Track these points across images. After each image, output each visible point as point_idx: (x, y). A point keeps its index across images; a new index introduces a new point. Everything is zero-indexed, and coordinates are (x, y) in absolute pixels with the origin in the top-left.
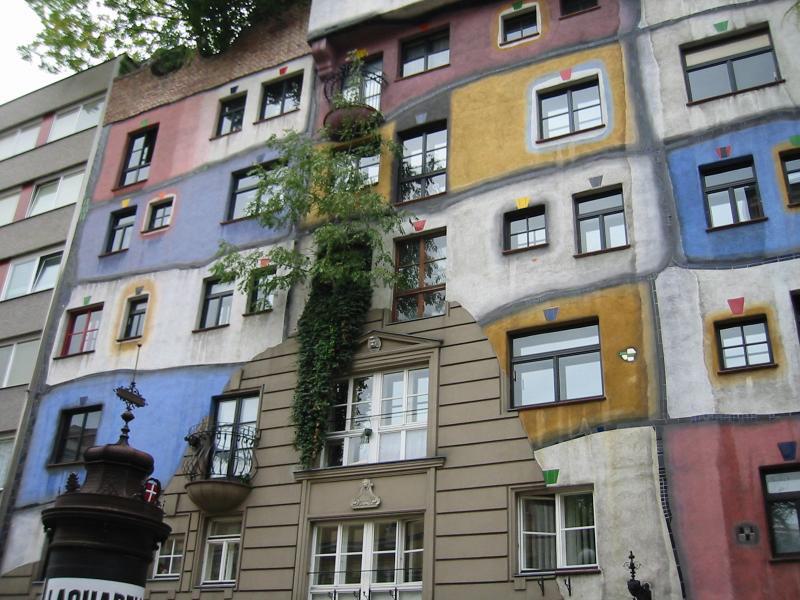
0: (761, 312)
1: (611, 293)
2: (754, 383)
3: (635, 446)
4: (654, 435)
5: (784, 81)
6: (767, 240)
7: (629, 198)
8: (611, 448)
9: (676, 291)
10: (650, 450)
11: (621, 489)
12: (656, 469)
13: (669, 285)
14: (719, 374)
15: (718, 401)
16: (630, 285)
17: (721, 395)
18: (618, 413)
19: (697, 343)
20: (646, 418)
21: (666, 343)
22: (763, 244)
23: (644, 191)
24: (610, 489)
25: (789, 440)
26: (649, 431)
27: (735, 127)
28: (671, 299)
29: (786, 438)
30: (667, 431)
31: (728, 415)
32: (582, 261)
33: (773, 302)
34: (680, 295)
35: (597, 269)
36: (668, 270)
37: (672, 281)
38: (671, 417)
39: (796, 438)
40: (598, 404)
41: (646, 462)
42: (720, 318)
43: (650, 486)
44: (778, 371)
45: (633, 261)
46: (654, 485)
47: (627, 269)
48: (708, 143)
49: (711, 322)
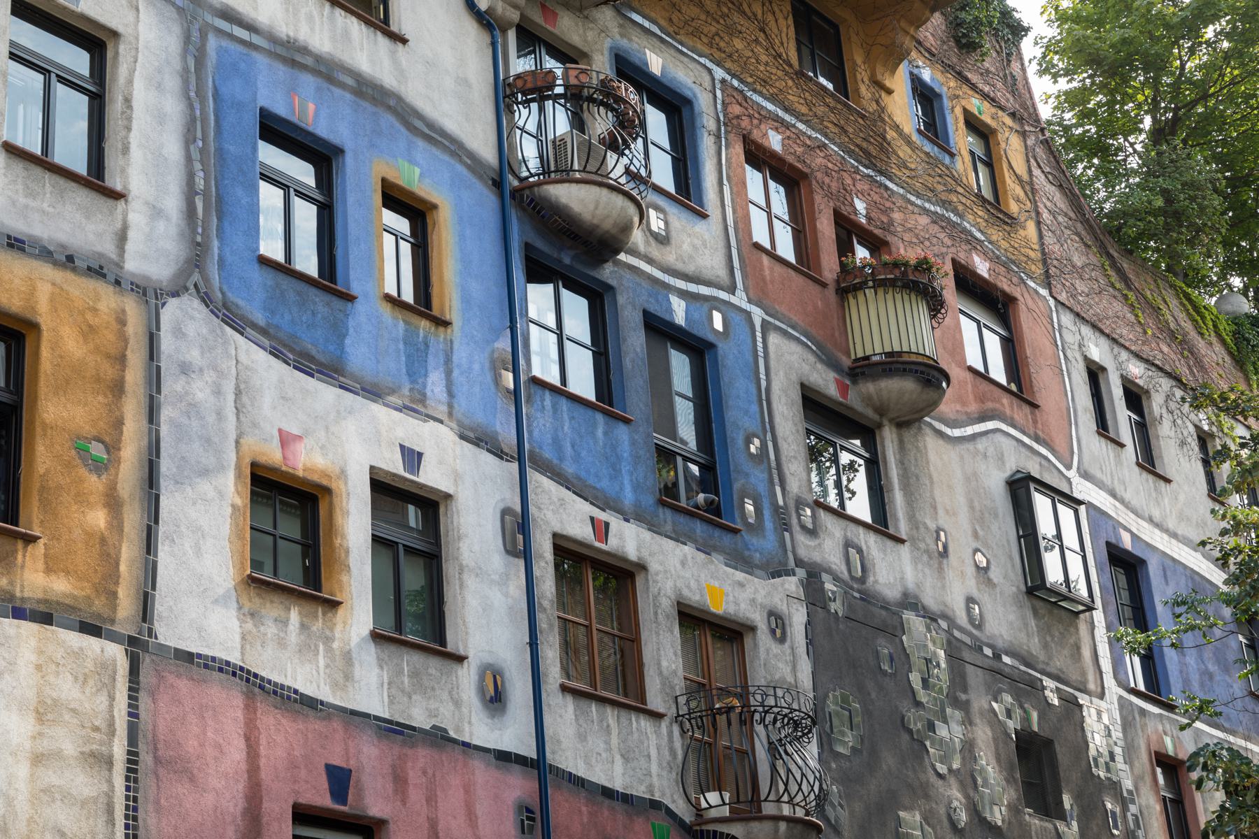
0: (325, 482)
1: (79, 287)
2: (303, 627)
3: (85, 682)
4: (123, 665)
5: (404, 41)
6: (348, 341)
7: (130, 82)
8: (39, 667)
9: (194, 355)
10: (112, 698)
11: (51, 777)
12: (119, 750)
13: (184, 334)
14: (252, 581)
15: (243, 638)
16: (111, 288)
17: (249, 625)
18: (60, 586)
19: (221, 495)
20: (113, 621)
21: (166, 466)
22: (342, 336)
23: (159, 87)
24: (23, 771)
25: (343, 765)
26: (116, 652)
27: (327, 71)
28: (185, 369)
29: (337, 761)
30: (146, 662)
31: (256, 676)
32: (19, 167)
33: (343, 473)
34: (201, 370)
35: (45, 205)
36: (185, 298)
37: (191, 329)
38: (161, 640)
39: (352, 764)
40: (20, 544)
41: (103, 726)
42: (262, 460)
43: (105, 787)
44: (341, 611)
45: (122, 238)
46: (110, 782)
47: (107, 247)
48: (282, 70)
49: (248, 461)
